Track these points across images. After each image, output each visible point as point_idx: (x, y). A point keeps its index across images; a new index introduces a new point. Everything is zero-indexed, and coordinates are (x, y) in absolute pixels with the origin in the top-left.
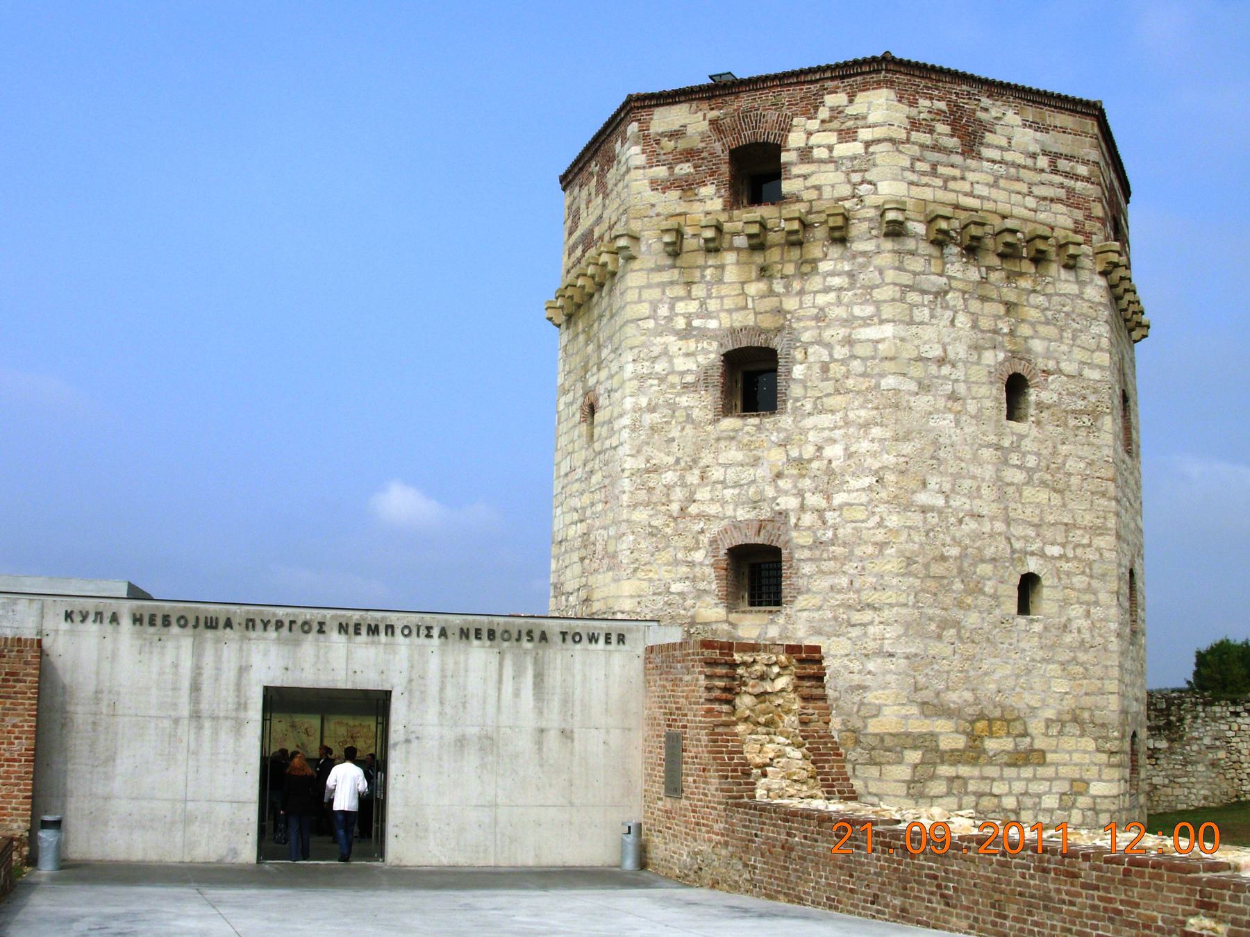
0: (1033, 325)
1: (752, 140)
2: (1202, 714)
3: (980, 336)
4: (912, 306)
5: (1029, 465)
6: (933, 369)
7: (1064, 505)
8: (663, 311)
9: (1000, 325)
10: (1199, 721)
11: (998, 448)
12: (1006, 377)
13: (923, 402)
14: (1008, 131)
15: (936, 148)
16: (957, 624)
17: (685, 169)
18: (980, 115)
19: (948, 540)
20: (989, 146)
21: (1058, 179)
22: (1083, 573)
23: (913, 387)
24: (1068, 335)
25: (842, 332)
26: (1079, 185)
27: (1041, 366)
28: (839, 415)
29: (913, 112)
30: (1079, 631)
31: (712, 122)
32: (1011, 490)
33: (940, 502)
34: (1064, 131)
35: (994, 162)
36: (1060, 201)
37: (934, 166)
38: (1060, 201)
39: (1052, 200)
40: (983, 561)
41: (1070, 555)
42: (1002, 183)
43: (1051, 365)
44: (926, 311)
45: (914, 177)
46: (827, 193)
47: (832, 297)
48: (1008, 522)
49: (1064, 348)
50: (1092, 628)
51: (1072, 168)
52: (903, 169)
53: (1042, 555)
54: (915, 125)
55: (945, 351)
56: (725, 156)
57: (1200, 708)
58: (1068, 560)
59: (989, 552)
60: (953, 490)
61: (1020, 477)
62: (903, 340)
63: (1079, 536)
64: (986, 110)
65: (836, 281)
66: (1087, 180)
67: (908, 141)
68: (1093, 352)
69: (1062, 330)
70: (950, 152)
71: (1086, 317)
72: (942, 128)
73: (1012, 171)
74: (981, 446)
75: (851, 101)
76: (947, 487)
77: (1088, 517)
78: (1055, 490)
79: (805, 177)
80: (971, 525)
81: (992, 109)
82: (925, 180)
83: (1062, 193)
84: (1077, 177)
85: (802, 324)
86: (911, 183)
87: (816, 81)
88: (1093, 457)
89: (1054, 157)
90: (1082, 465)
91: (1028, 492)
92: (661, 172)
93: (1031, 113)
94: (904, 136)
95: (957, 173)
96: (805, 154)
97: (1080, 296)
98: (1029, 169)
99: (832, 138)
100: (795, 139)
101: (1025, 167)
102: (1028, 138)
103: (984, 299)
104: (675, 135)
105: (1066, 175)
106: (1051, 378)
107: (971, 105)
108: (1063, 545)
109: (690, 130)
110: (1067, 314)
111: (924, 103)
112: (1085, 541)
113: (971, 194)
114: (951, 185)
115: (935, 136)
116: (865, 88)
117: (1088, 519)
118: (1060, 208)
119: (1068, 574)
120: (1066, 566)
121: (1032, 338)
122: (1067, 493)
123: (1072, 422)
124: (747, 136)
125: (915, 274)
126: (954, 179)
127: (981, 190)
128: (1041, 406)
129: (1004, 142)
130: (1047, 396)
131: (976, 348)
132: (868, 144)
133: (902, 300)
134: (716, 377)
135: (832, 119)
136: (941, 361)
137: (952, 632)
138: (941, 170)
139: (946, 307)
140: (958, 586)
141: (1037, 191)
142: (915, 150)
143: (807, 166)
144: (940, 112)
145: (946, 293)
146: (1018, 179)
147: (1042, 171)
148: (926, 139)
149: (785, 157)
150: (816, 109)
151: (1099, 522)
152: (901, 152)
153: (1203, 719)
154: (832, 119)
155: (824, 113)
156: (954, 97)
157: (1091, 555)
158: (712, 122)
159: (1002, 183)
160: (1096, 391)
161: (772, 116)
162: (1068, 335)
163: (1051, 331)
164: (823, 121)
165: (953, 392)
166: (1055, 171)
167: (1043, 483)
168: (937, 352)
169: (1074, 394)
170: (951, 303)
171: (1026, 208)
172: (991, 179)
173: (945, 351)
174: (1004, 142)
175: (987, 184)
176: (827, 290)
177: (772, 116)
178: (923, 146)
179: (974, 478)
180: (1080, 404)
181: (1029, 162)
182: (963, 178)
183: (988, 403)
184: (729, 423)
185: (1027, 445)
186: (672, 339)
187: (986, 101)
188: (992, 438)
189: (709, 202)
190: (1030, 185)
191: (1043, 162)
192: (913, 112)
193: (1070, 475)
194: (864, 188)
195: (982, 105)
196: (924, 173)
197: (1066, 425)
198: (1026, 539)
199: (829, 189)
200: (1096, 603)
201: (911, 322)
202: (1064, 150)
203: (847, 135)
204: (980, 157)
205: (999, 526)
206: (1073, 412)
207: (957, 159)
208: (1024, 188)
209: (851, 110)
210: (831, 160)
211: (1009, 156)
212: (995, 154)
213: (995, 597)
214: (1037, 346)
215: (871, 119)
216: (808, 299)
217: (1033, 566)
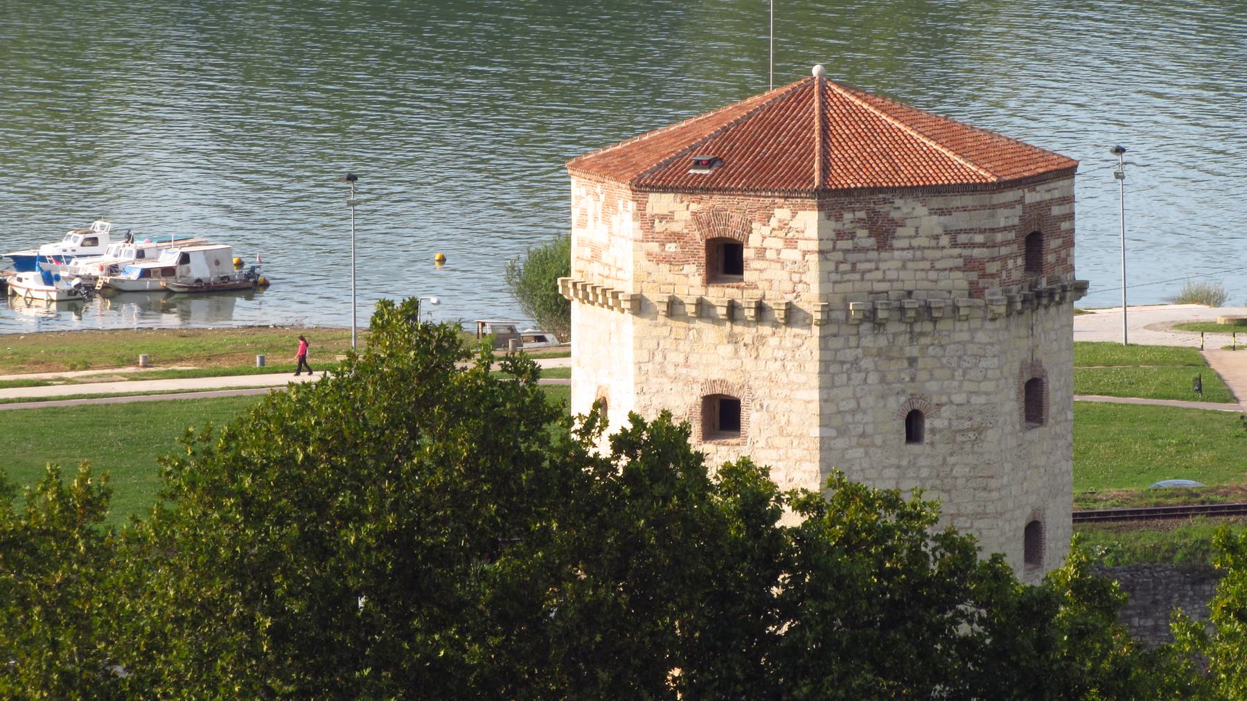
1: (723, 235)
2: (1191, 593)
3: (886, 387)
4: (833, 375)
5: (923, 476)
6: (849, 418)
7: (951, 501)
8: (659, 358)
9: (903, 376)
10: (1187, 599)
11: (899, 467)
12: (906, 413)
13: (840, 443)
14: (916, 222)
15: (856, 249)
17: (671, 248)
18: (895, 215)
20: (899, 238)
21: (957, 251)
23: (833, 433)
24: (958, 373)
25: (786, 391)
26: (976, 252)
27: (935, 400)
28: (781, 452)
29: (839, 226)
31: (694, 214)
34: (965, 209)
35: (903, 249)
36: (958, 268)
37: (854, 265)
38: (958, 268)
39: (951, 269)
42: (910, 265)
43: (944, 399)
44: (845, 376)
46: (776, 284)
47: (779, 363)
49: (956, 384)
51: (970, 239)
52: (829, 273)
54: (840, 235)
55: (858, 404)
56: (703, 243)
57: (1188, 587)
66: (983, 245)
67: (834, 249)
68: (980, 382)
71: (975, 356)
72: (862, 233)
73: (918, 254)
74: (885, 467)
75: (793, 217)
77: (970, 507)
78: (943, 491)
79: (761, 271)
81: (905, 207)
82: (846, 277)
83: (960, 262)
84: (973, 245)
85: (757, 382)
86: (835, 282)
87: (769, 197)
88: (976, 462)
89: (953, 233)
90: (967, 470)
92: (654, 247)
93: (937, 202)
94: (830, 245)
95: (872, 265)
96: (761, 253)
97: (972, 341)
98: (933, 248)
99: (779, 244)
100: (754, 240)
101: (929, 248)
102: (933, 223)
104: (662, 218)
105: (964, 246)
106: (944, 408)
107: (887, 207)
109: (676, 217)
111: (848, 216)
112: (968, 525)
113: (883, 280)
114: (868, 276)
115: (856, 240)
116: (804, 208)
117: (970, 508)
118: (960, 274)
121: (929, 381)
122: (953, 492)
123: (959, 438)
124: (717, 231)
126: (870, 271)
127: (892, 275)
128: (933, 431)
129: (912, 232)
130: (938, 424)
131: (882, 397)
132: (805, 253)
136: (853, 412)
141: (938, 265)
142: (839, 256)
143: (761, 262)
146: (923, 259)
147: (943, 248)
148: (848, 244)
149: (747, 253)
150: (769, 218)
151: (980, 510)
152: (827, 260)
153: (1191, 597)
155: (774, 223)
156: (872, 205)
158: (694, 214)
159: (910, 265)
160: (981, 412)
161: (737, 218)
162: (958, 373)
164: (774, 229)
165: (864, 432)
169: (962, 418)
170: (863, 367)
171: (928, 280)
172: (899, 264)
173: (858, 404)
174: (912, 232)
177: (737, 218)
178: (846, 251)
180: (967, 424)
181: (933, 243)
182: (877, 269)
185: (922, 461)
186: (665, 380)
187: (899, 202)
188: (894, 461)
189: (692, 278)
190: (933, 262)
191: (945, 241)
192: (839, 226)
193: (956, 478)
194: (800, 287)
195: (896, 205)
196: (845, 273)
197: (954, 441)
199: (777, 283)
202: (963, 226)
203: (791, 243)
204: (892, 248)
206: (960, 431)
207: (873, 255)
208: (927, 265)
209: (791, 224)
210: (778, 261)
211: (915, 243)
212: (904, 243)
214: (933, 386)
215: (806, 235)
216: (761, 363)
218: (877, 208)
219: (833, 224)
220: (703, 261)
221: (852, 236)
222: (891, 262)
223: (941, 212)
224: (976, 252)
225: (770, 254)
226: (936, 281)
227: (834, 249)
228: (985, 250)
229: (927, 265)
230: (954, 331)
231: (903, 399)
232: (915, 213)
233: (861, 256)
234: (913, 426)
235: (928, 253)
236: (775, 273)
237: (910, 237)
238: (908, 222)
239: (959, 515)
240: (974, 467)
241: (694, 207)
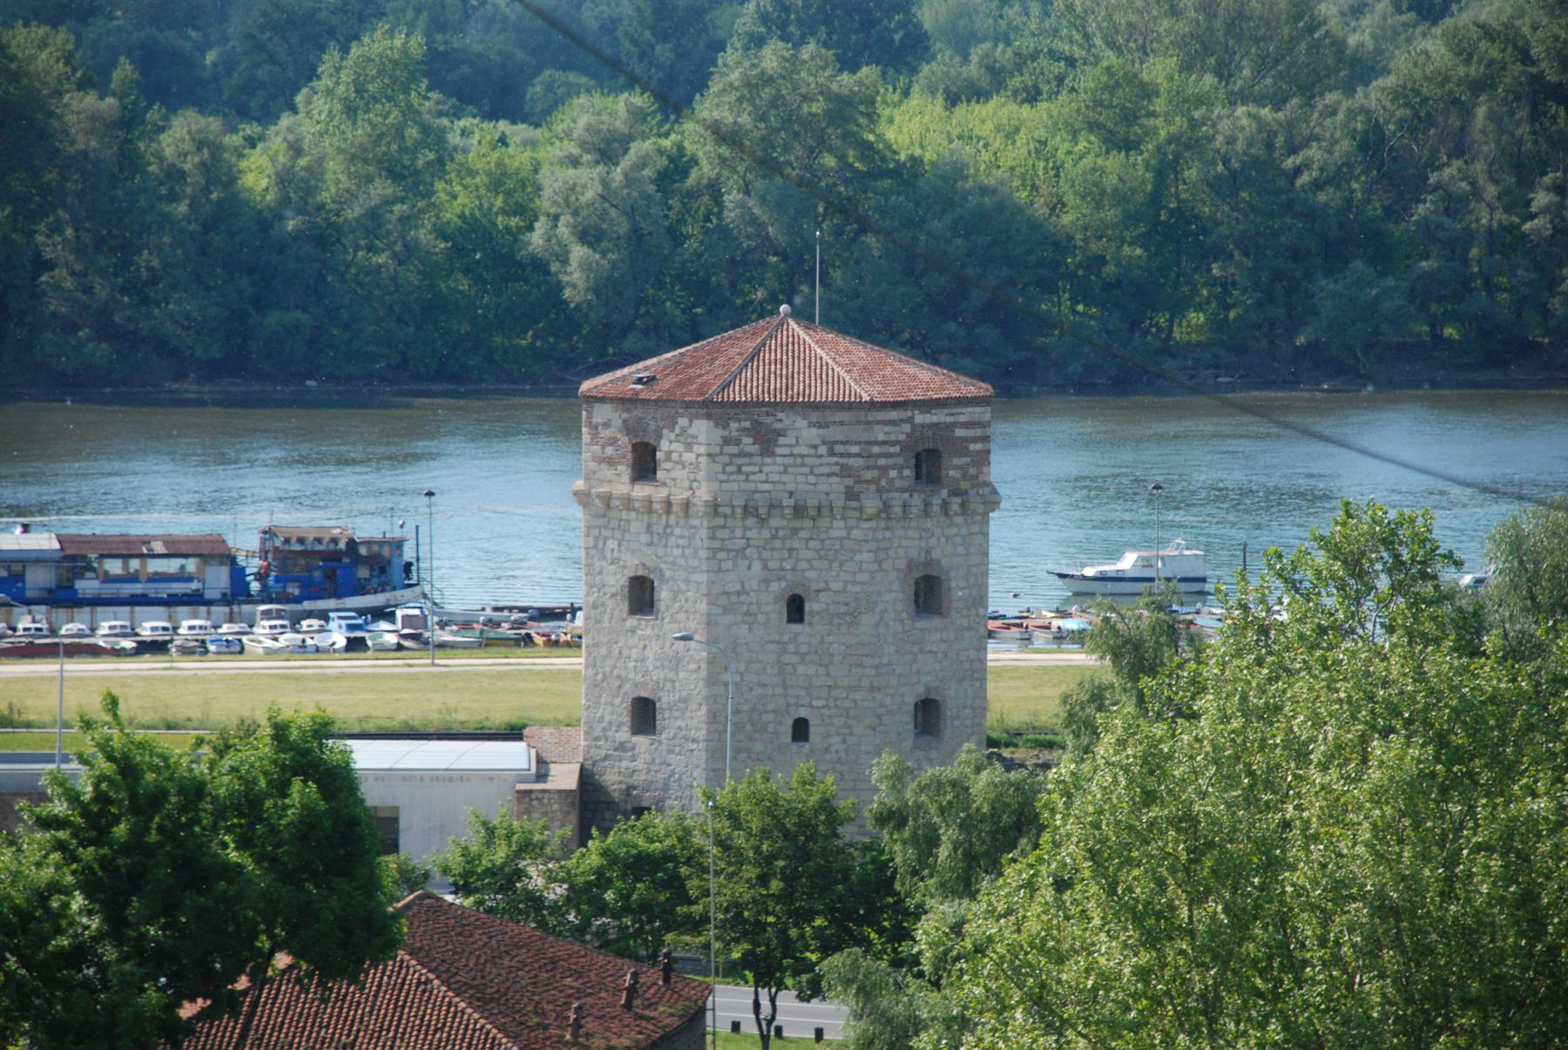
0: (809, 561)
4: (721, 561)
6: (734, 598)
7: (828, 675)
9: (784, 564)
12: (787, 596)
13: (727, 619)
15: (742, 454)
16: (748, 750)
18: (777, 426)
19: (742, 701)
20: (781, 446)
21: (834, 459)
22: (841, 716)
23: (720, 611)
24: (836, 565)
26: (852, 462)
27: (814, 586)
29: (726, 433)
30: (837, 751)
32: (788, 668)
33: (737, 678)
34: (842, 423)
35: (785, 456)
37: (739, 467)
39: (828, 475)
40: (766, 712)
41: (831, 703)
42: (790, 469)
43: (822, 585)
44: (730, 563)
45: (724, 477)
48: (785, 687)
49: (834, 573)
50: (847, 751)
52: (717, 473)
53: (810, 706)
54: (727, 441)
58: (830, 708)
59: (771, 707)
60: (746, 670)
61: (796, 659)
62: (713, 583)
63: (836, 693)
64: (781, 421)
65: (681, 542)
66: (859, 455)
67: (721, 453)
69: (831, 562)
70: (751, 455)
71: (851, 550)
72: (747, 440)
73: (799, 460)
76: (742, 669)
79: (668, 470)
80: (758, 691)
81: (785, 419)
82: (732, 477)
83: (837, 469)
84: (850, 455)
89: (831, 445)
91: (801, 669)
93: (815, 416)
94: (717, 450)
97: (848, 537)
100: (664, 445)
102: (812, 435)
103: (772, 550)
105: (841, 455)
107: (771, 419)
108: (827, 699)
110: (836, 551)
111: (734, 425)
113: (766, 482)
114: (752, 477)
116: (697, 417)
117: (846, 682)
118: (836, 479)
119: (830, 717)
120: (826, 712)
123: (836, 621)
125: (723, 540)
128: (812, 613)
129: (793, 441)
133: (714, 557)
134: (626, 591)
135: (681, 435)
136: (738, 593)
137: (745, 755)
138: (744, 469)
139: (744, 557)
140: (749, 728)
141: (816, 471)
142: (726, 459)
144: (745, 429)
145: (745, 549)
146: (803, 465)
148: (734, 449)
154: (681, 435)
155: (677, 430)
157: (847, 704)
159: (790, 469)
162: (836, 565)
163: (825, 564)
166: (831, 453)
167: (811, 662)
168: (738, 587)
172: (782, 468)
174: (793, 441)
175: (780, 473)
176: (678, 546)
179: (761, 662)
181: (813, 452)
182: (761, 472)
183: (773, 616)
184: (632, 622)
185: (801, 639)
187: (780, 415)
190: (812, 468)
191: (823, 450)
196: (732, 473)
197: (831, 623)
198: (798, 697)
200: (851, 734)
201: (720, 570)
202: (839, 438)
203: (689, 447)
204: (774, 455)
205: (779, 690)
206: (838, 614)
207: (757, 459)
208: (807, 470)
209: (690, 431)
211: (796, 450)
212: (786, 451)
213: (776, 733)
214: (811, 574)
217: (803, 713)
218: (762, 419)
219: (720, 432)
220: (630, 462)
221: (738, 443)
222: (772, 467)
223: (819, 425)
224: (852, 462)
225: (674, 456)
226: (815, 484)
227: (721, 453)
228: (860, 460)
229: (807, 470)
230: (832, 528)
231: (783, 584)
232: (796, 425)
233: (747, 460)
234: (796, 608)
235: (808, 461)
236: (681, 474)
237: (791, 446)
238: (789, 432)
239: (836, 687)
240: (849, 647)
241: (625, 416)
